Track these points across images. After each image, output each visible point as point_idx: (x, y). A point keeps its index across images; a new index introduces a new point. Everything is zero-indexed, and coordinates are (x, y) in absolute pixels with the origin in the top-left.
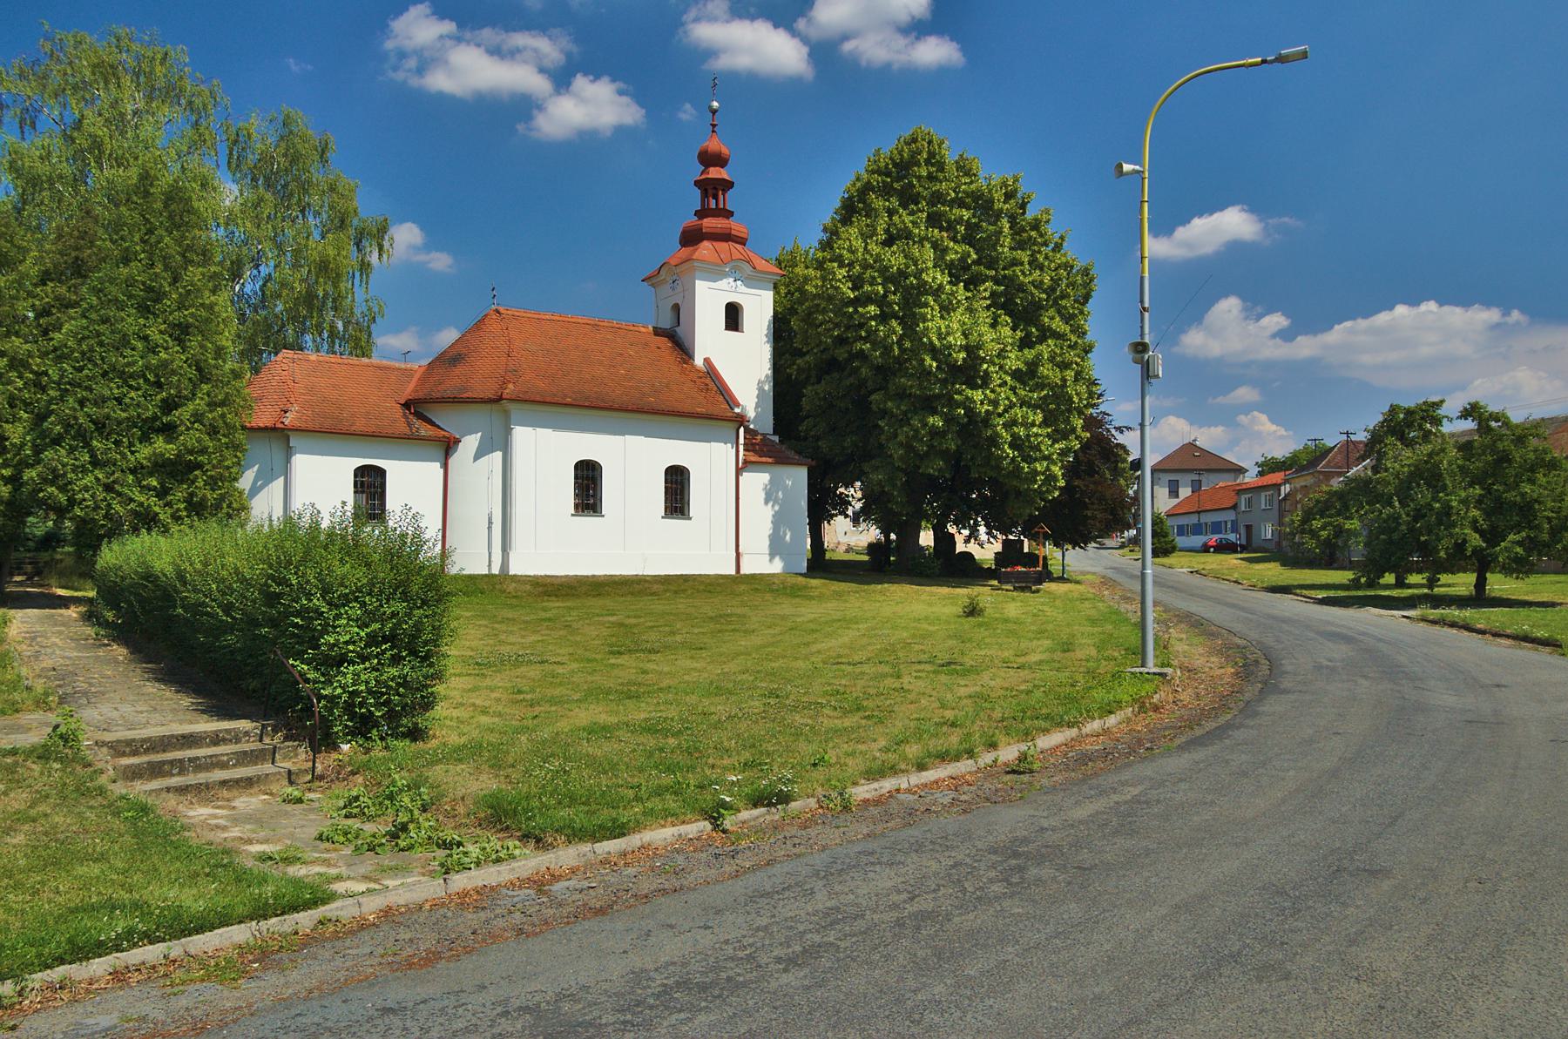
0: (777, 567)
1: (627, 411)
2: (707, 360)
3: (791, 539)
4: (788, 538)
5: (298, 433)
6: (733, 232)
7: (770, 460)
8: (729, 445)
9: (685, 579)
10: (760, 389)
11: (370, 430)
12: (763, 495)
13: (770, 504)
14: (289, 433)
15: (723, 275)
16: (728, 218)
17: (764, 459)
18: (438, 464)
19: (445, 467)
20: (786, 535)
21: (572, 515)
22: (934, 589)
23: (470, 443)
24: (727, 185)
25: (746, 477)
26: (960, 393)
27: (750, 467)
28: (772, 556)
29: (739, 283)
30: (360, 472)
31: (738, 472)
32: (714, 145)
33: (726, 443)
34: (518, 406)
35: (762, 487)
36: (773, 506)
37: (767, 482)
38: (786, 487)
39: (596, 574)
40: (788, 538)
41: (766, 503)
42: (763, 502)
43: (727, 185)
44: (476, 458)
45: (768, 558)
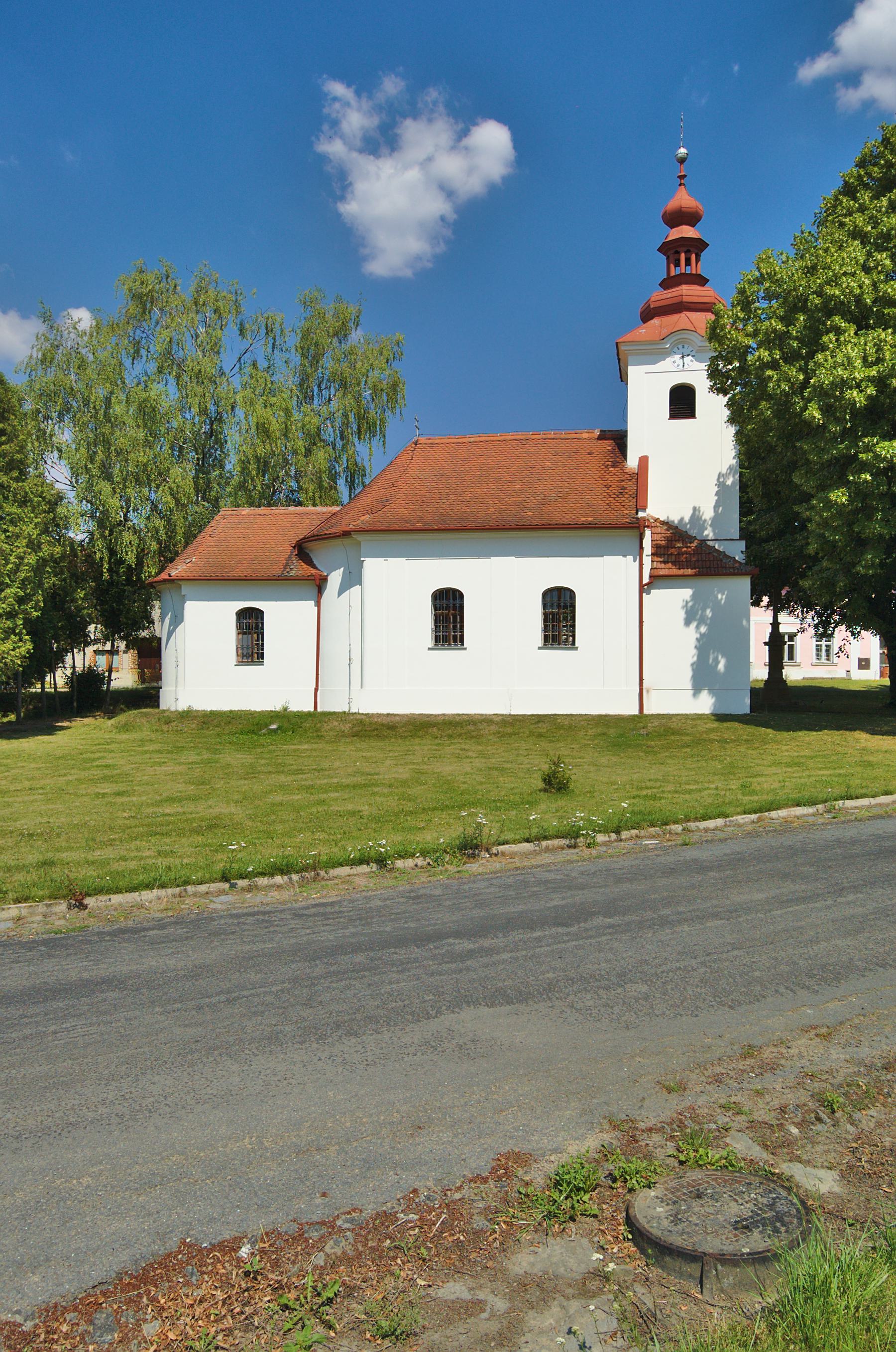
0: (704, 704)
1: (491, 529)
2: (644, 461)
3: (726, 667)
4: (721, 666)
5: (189, 582)
6: (685, 299)
7: (689, 571)
8: (630, 558)
9: (540, 719)
10: (721, 485)
11: (249, 573)
12: (682, 615)
13: (693, 625)
14: (180, 583)
15: (663, 354)
16: (703, 285)
17: (681, 572)
18: (312, 603)
19: (318, 604)
20: (718, 663)
21: (539, 648)
22: (40, 737)
23: (335, 579)
24: (697, 246)
25: (658, 597)
26: (868, 449)
27: (657, 582)
28: (697, 689)
29: (688, 359)
30: (243, 614)
31: (643, 589)
32: (683, 199)
33: (625, 556)
34: (367, 537)
35: (681, 604)
36: (698, 627)
37: (689, 599)
38: (717, 603)
39: (214, 709)
40: (721, 666)
41: (687, 623)
42: (682, 622)
43: (697, 246)
44: (340, 593)
45: (691, 692)
